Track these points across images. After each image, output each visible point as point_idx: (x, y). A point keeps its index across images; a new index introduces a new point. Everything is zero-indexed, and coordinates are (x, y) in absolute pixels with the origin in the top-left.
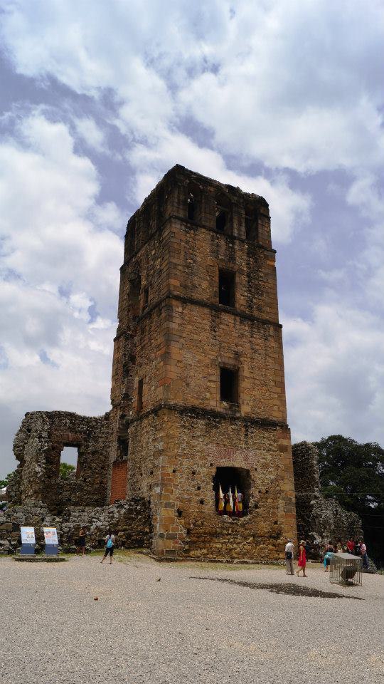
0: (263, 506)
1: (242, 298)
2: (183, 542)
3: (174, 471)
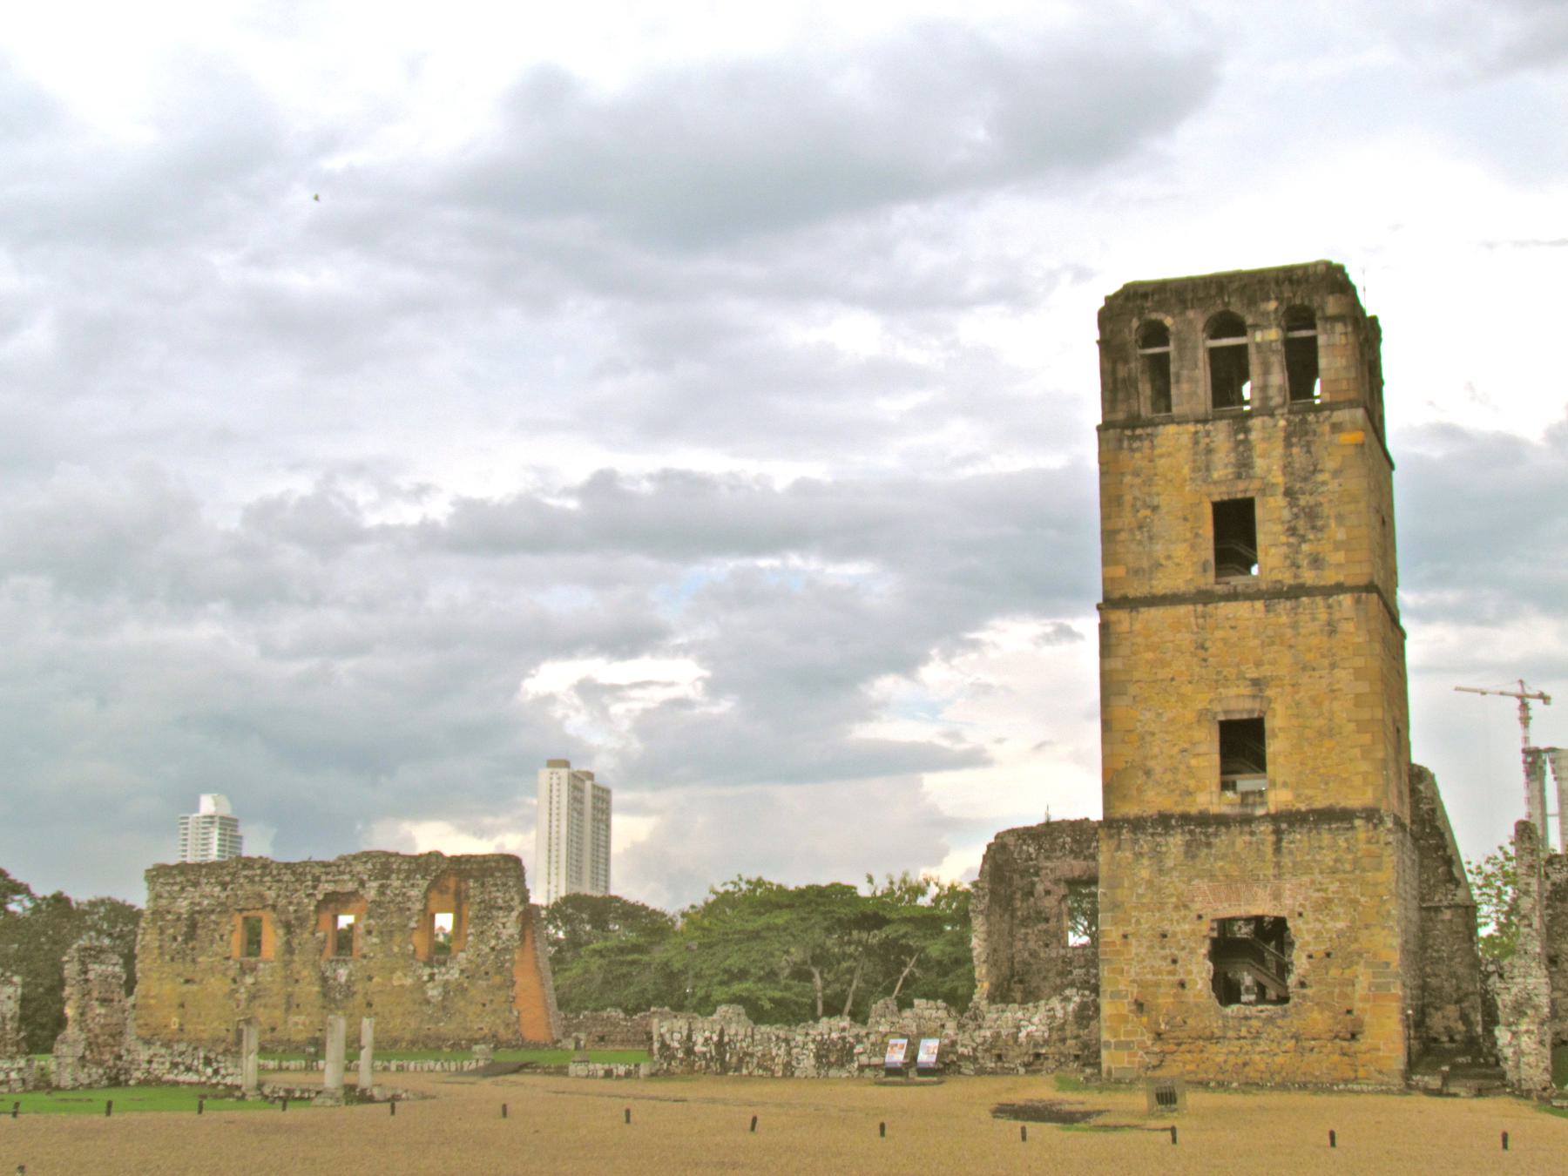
0: (1319, 982)
1: (1273, 551)
2: (1147, 1053)
3: (1125, 936)
